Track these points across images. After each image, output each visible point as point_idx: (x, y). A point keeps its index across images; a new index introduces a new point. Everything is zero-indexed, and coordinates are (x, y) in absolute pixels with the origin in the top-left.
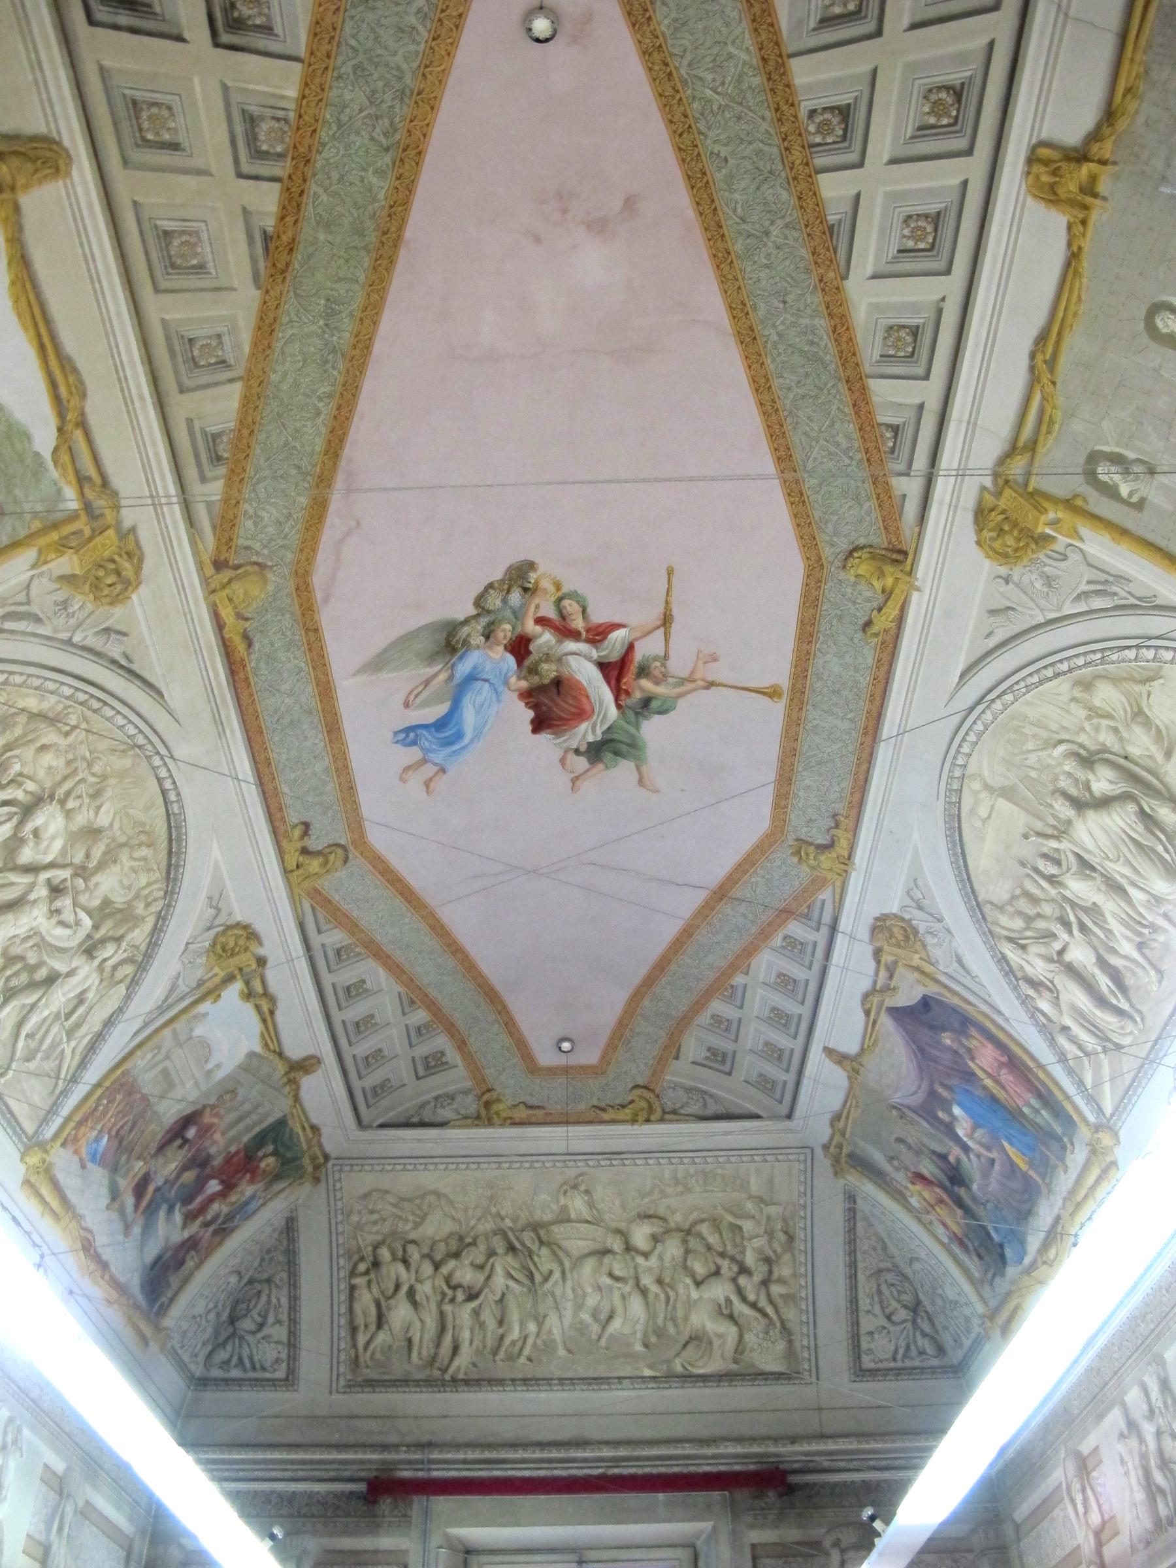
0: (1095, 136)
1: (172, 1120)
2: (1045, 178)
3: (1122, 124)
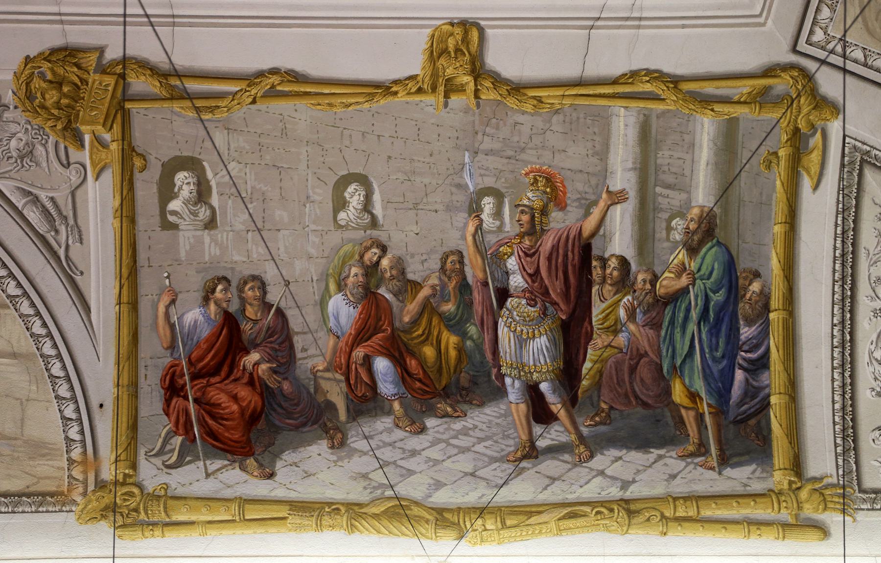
0: (497, 80)
2: (451, 43)
3: (511, 102)
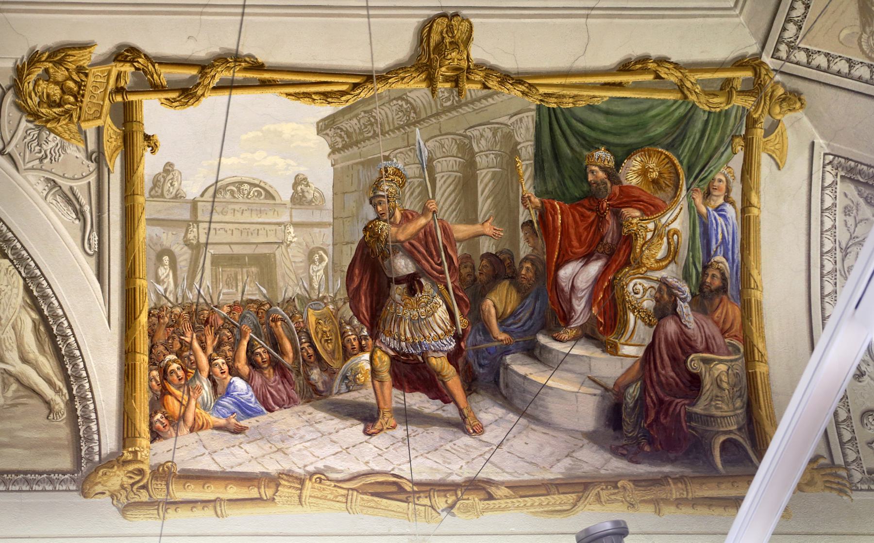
1: (339, 283)
